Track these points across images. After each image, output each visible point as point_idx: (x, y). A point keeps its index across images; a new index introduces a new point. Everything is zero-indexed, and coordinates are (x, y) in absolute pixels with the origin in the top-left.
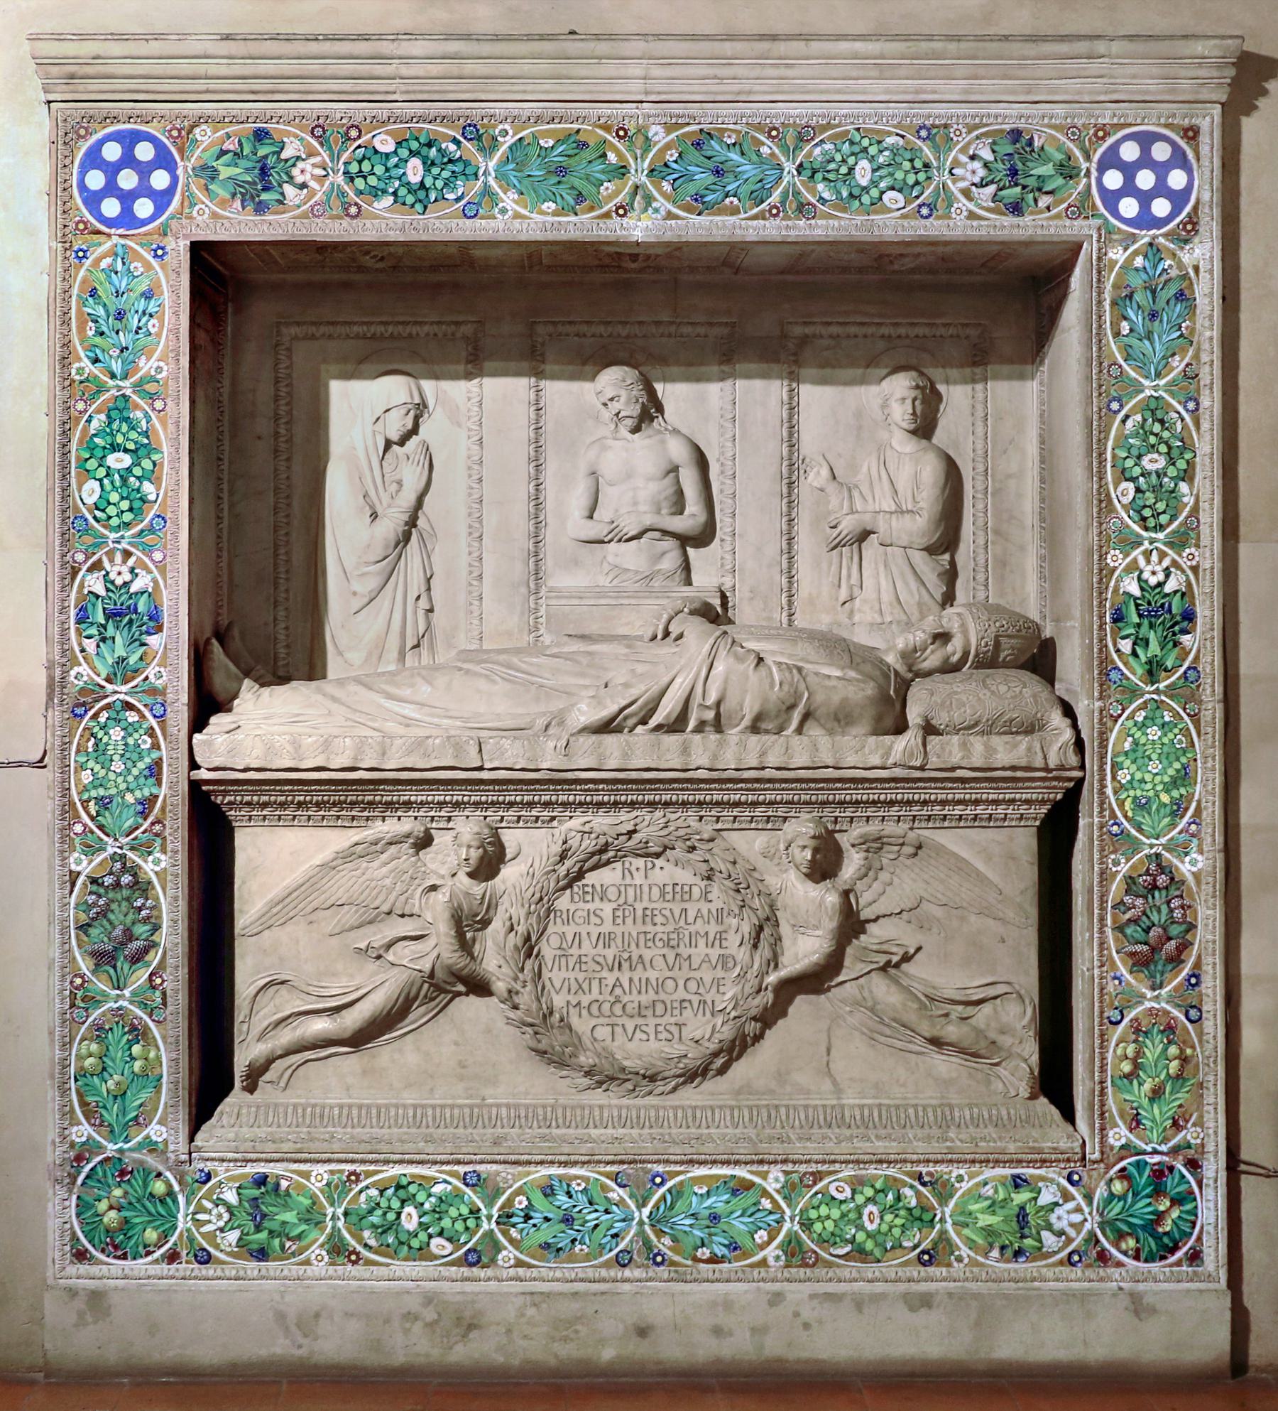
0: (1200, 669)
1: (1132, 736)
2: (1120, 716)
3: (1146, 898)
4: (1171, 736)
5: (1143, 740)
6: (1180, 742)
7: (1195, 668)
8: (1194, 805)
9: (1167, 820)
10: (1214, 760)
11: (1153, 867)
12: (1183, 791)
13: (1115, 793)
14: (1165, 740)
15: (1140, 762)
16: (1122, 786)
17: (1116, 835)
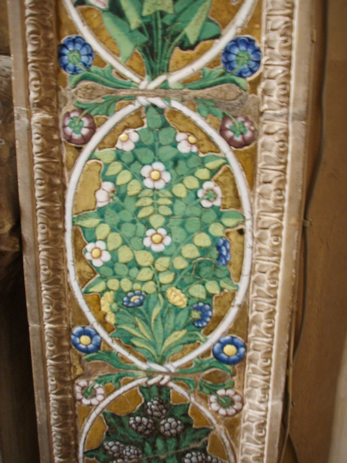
0: (260, 44)
1: (113, 179)
2: (86, 140)
3: (140, 446)
4: (191, 182)
5: (134, 188)
6: (211, 195)
7: (249, 43)
8: (233, 313)
9: (180, 334)
10: (277, 236)
11: (153, 404)
12: (212, 287)
13: (83, 281)
14: (180, 190)
15: (128, 229)
16: (95, 271)
17: (87, 351)
